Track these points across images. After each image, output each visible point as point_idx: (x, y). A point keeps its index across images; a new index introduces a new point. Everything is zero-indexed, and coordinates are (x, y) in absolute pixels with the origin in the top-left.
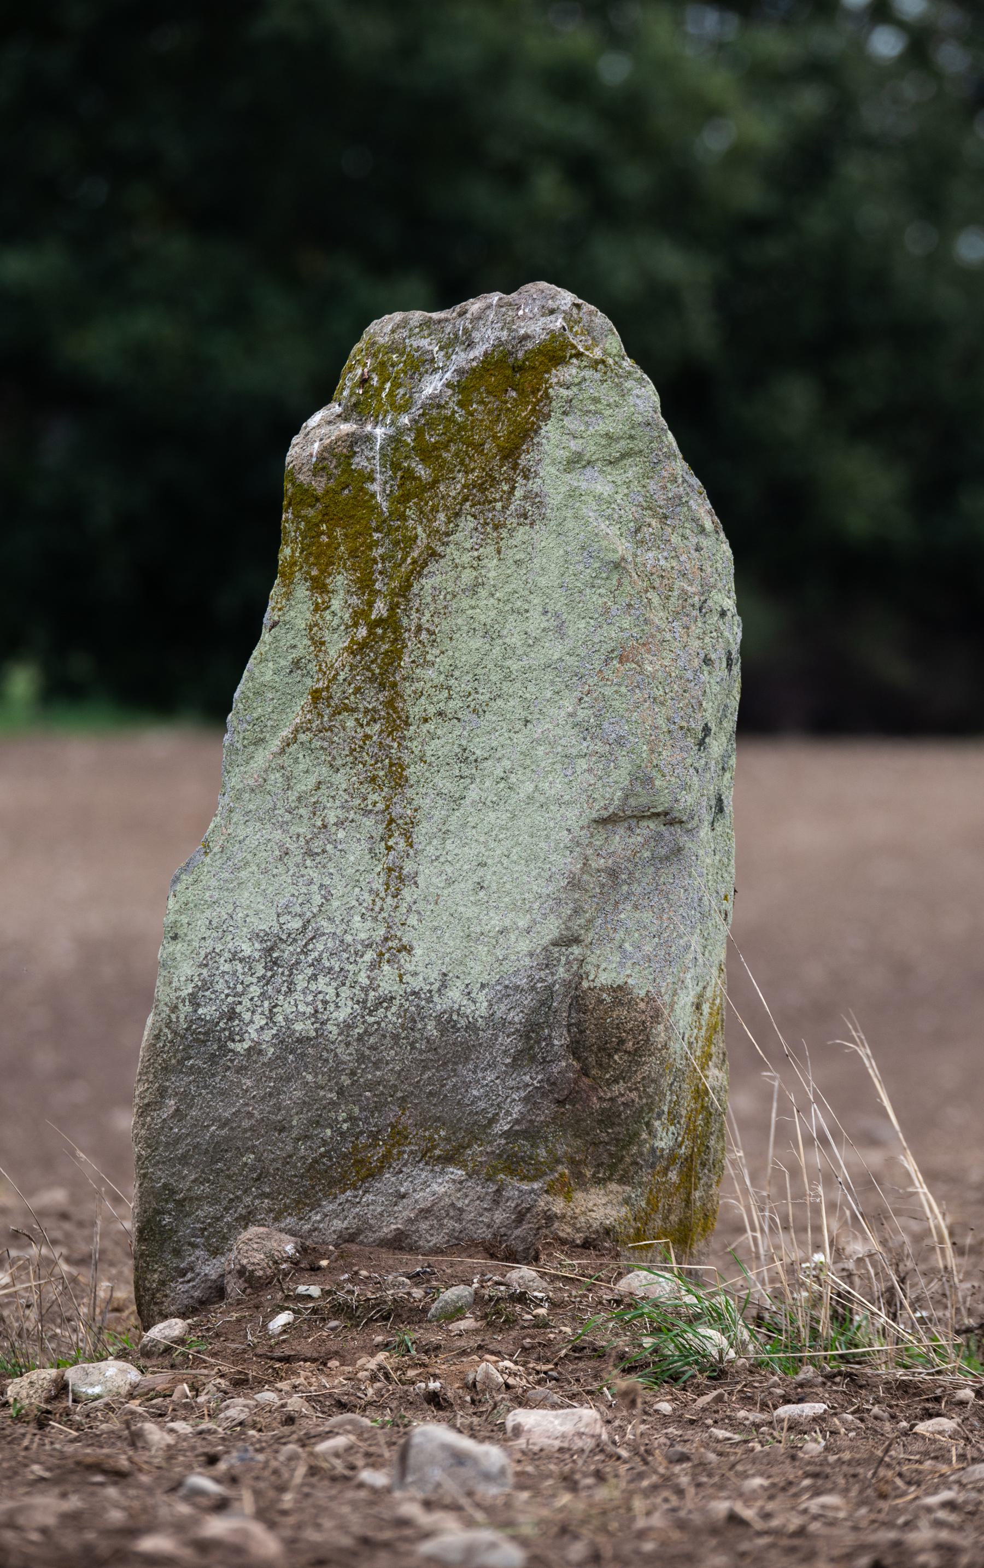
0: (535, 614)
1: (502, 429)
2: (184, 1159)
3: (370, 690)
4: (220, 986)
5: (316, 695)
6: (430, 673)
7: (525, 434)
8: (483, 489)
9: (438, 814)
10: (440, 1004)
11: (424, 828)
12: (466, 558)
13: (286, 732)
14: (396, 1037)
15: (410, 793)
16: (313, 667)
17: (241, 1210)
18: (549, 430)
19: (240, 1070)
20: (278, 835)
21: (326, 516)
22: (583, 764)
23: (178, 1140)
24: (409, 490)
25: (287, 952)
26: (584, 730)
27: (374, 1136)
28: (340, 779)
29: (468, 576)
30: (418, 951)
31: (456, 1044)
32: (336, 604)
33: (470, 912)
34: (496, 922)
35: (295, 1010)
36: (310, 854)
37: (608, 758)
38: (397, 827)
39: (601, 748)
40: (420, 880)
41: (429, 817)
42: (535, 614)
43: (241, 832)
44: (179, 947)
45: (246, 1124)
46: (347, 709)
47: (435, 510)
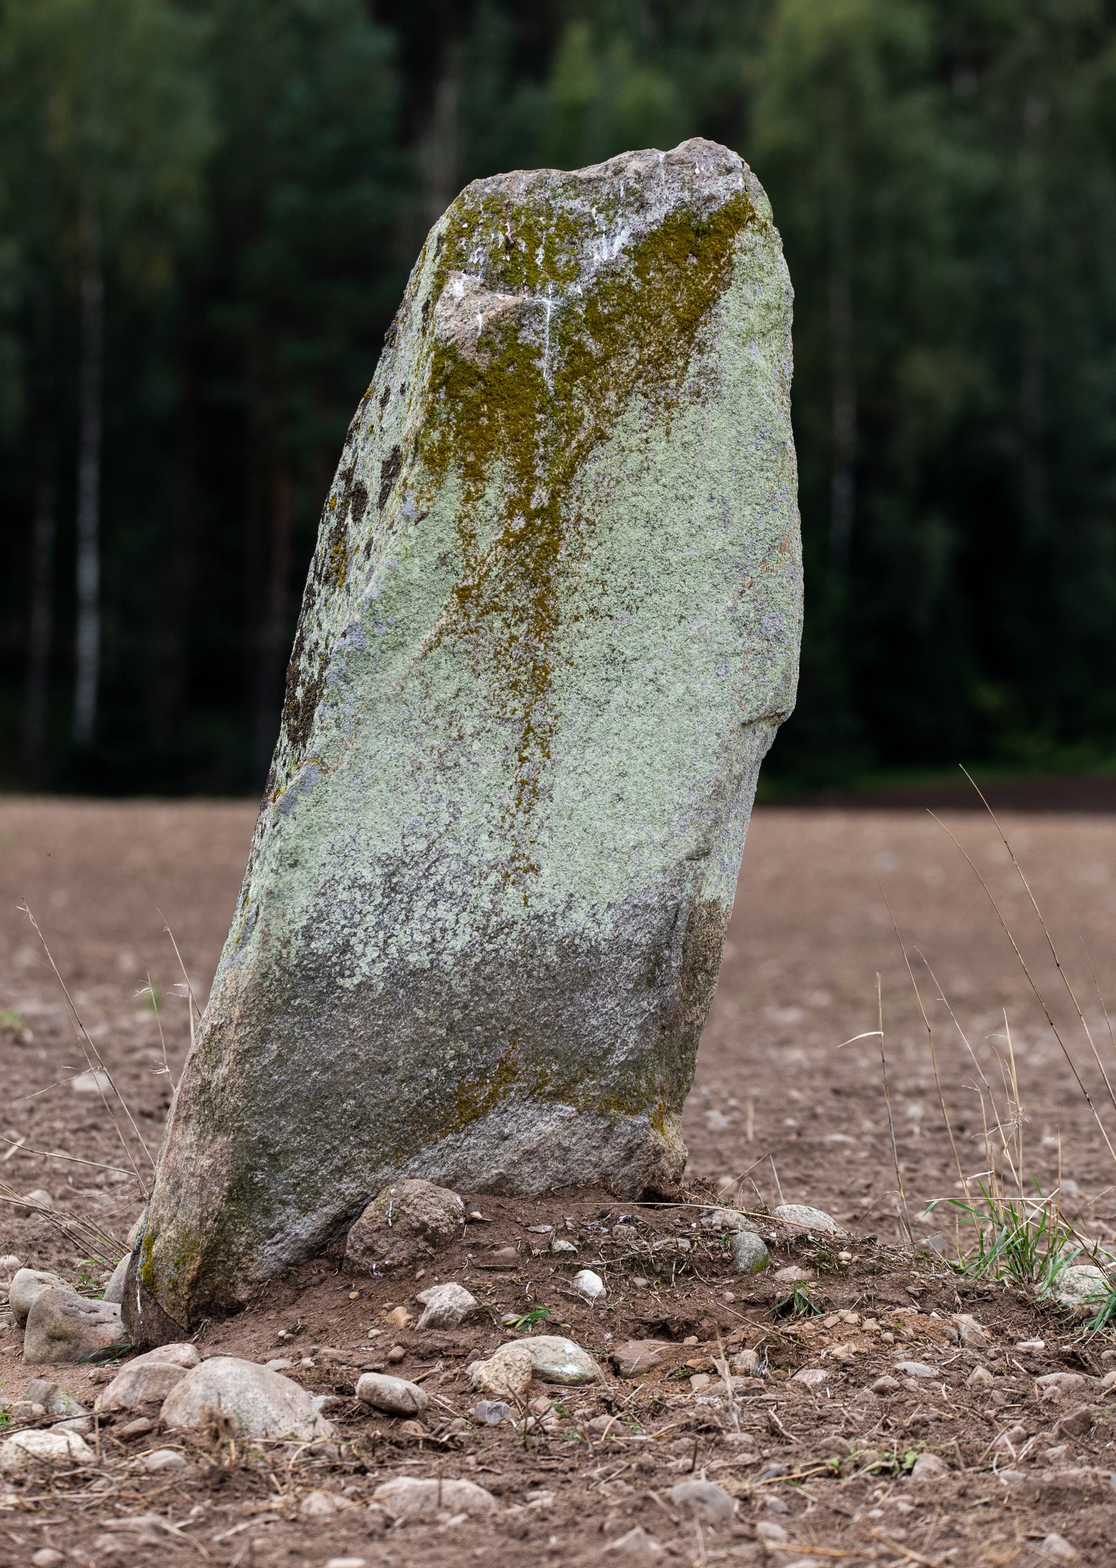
0: (701, 501)
1: (681, 299)
2: (282, 1110)
3: (521, 588)
4: (337, 916)
5: (463, 594)
6: (585, 567)
7: (705, 303)
8: (657, 365)
9: (580, 721)
10: (563, 928)
11: (565, 736)
12: (634, 441)
13: (429, 635)
14: (513, 965)
15: (552, 698)
16: (459, 563)
17: (338, 1162)
18: (728, 298)
19: (348, 1008)
20: (410, 748)
21: (488, 396)
22: (737, 662)
23: (278, 1087)
24: (578, 366)
25: (408, 877)
26: (743, 626)
27: (482, 1074)
28: (480, 686)
29: (634, 461)
30: (546, 871)
31: (577, 970)
32: (491, 493)
33: (605, 826)
34: (631, 837)
35: (410, 940)
36: (442, 768)
37: (766, 656)
38: (535, 736)
39: (758, 644)
40: (556, 794)
41: (570, 724)
42: (701, 501)
43: (373, 746)
44: (298, 874)
45: (350, 1067)
46: (497, 608)
47: (605, 388)
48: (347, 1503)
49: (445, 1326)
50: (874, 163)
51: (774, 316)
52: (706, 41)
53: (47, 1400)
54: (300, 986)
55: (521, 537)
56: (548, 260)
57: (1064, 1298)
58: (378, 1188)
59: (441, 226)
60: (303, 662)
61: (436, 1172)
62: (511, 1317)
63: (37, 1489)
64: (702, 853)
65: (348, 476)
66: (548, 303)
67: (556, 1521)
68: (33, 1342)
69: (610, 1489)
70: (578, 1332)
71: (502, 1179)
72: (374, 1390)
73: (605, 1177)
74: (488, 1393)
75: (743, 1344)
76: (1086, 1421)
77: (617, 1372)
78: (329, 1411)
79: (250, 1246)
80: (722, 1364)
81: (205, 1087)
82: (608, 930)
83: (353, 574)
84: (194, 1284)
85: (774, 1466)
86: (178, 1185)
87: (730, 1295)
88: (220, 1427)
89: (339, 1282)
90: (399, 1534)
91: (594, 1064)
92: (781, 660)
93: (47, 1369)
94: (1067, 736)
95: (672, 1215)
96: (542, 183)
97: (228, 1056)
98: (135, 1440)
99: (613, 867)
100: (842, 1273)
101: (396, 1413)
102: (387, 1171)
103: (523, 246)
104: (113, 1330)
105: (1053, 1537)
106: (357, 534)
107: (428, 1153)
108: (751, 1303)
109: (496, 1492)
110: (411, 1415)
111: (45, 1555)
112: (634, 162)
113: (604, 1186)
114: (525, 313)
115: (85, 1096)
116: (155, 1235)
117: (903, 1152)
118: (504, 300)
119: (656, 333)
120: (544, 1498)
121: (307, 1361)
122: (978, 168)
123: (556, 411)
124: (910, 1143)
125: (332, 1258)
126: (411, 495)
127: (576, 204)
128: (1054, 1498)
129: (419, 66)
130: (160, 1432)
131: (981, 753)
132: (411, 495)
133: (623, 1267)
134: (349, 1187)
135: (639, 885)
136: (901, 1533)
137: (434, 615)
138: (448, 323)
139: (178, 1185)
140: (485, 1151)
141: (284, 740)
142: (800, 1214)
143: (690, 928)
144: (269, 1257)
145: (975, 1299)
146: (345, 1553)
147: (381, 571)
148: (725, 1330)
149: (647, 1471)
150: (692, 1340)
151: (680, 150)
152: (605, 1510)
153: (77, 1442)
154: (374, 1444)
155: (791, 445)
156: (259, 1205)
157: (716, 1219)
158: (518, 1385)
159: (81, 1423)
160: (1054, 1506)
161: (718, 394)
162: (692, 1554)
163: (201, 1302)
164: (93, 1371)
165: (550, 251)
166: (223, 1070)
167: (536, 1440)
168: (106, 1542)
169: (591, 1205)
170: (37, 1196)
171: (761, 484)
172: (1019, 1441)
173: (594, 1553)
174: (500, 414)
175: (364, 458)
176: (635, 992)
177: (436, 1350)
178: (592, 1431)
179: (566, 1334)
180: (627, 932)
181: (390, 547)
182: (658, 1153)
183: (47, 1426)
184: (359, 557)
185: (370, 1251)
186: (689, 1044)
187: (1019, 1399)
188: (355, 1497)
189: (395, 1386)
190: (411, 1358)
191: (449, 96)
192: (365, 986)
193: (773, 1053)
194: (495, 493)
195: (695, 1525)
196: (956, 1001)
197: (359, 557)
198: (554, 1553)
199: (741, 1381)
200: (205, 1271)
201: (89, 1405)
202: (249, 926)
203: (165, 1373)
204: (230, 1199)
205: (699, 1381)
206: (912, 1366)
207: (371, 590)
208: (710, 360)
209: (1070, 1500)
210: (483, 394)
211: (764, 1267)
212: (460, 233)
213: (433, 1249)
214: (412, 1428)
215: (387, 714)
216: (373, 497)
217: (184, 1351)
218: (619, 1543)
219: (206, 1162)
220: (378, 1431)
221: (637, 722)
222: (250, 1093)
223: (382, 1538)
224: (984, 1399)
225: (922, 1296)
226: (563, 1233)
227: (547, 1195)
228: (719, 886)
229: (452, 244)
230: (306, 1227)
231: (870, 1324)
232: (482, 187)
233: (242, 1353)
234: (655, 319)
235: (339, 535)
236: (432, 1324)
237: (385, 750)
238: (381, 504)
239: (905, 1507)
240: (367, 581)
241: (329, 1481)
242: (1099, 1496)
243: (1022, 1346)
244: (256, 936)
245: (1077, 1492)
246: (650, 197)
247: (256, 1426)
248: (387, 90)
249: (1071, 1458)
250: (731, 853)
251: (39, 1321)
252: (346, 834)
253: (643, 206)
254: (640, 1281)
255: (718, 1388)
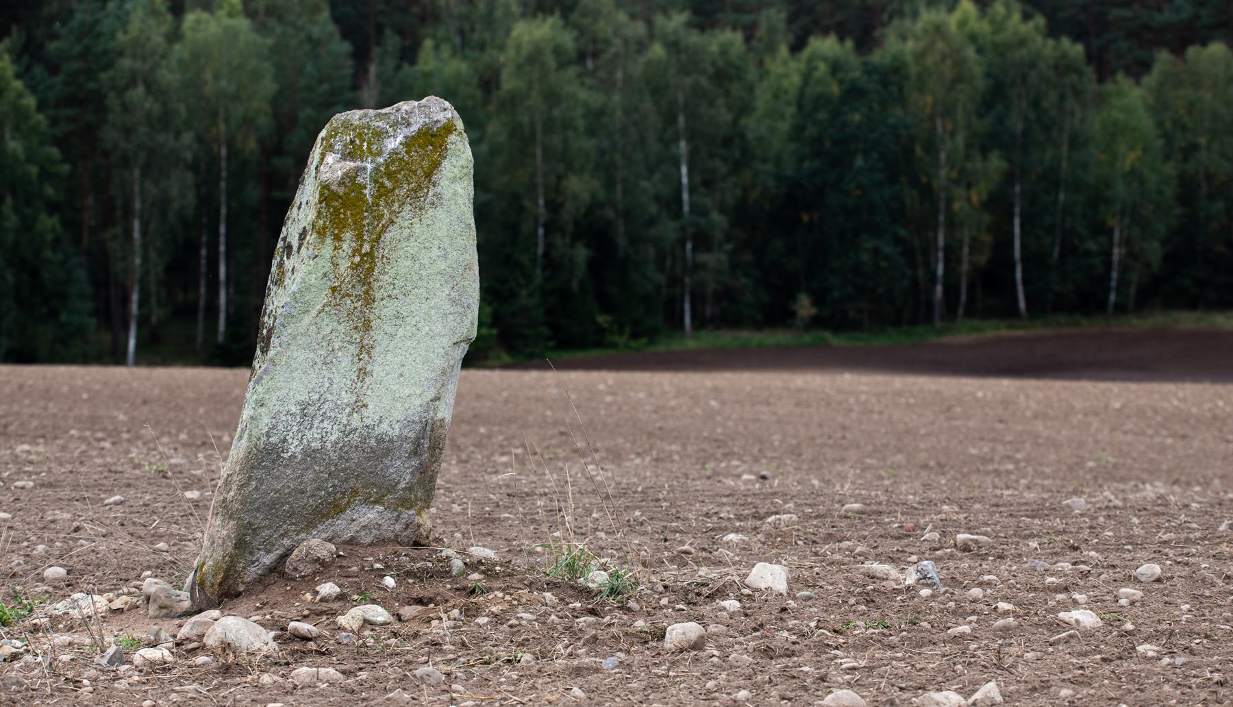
0: (435, 249)
1: (425, 164)
2: (258, 510)
3: (358, 287)
4: (280, 427)
5: (334, 289)
6: (386, 277)
7: (436, 165)
8: (416, 192)
9: (385, 343)
10: (378, 431)
11: (378, 349)
12: (406, 224)
13: (319, 307)
14: (357, 447)
15: (372, 333)
16: (332, 276)
17: (282, 532)
18: (445, 163)
19: (286, 466)
20: (312, 355)
21: (343, 205)
22: (451, 317)
23: (256, 500)
24: (382, 192)
25: (311, 410)
26: (453, 302)
27: (343, 493)
28: (342, 328)
29: (406, 232)
30: (370, 407)
31: (384, 449)
32: (345, 246)
33: (395, 387)
34: (407, 392)
35: (312, 437)
36: (325, 364)
37: (463, 314)
38: (365, 349)
39: (460, 310)
40: (374, 374)
41: (380, 344)
42: (435, 249)
43: (295, 354)
44: (264, 409)
45: (287, 491)
46: (348, 295)
47: (393, 201)
48: (279, 678)
49: (327, 601)
50: (552, 97)
51: (465, 170)
52: (482, 47)
53: (157, 634)
54: (265, 457)
55: (358, 265)
56: (368, 148)
57: (590, 585)
58: (299, 542)
59: (323, 133)
60: (266, 319)
61: (324, 535)
62: (355, 597)
63: (148, 673)
64: (437, 399)
65: (284, 239)
66: (369, 166)
67: (367, 685)
68: (152, 609)
69: (392, 671)
70: (384, 603)
71: (353, 538)
72: (296, 629)
73: (396, 536)
74: (344, 629)
75: (454, 607)
76: (595, 638)
77: (400, 620)
78: (276, 638)
79: (244, 568)
80: (443, 615)
81: (224, 501)
82: (397, 432)
83: (287, 281)
84: (220, 584)
85: (462, 660)
86: (213, 542)
87: (449, 586)
88: (226, 647)
89: (282, 582)
90: (299, 692)
91: (392, 488)
92: (470, 316)
93: (158, 621)
94: (635, 336)
95: (425, 552)
96: (366, 115)
97: (234, 487)
98: (193, 652)
99: (399, 405)
100: (497, 576)
101: (305, 639)
102: (303, 535)
103: (358, 142)
104: (187, 604)
105: (575, 689)
106: (289, 264)
107: (321, 527)
108: (457, 589)
109: (344, 673)
110: (310, 640)
111: (148, 703)
112: (404, 106)
113: (396, 540)
114: (359, 170)
115: (189, 500)
116: (204, 564)
117: (533, 521)
118: (350, 164)
119: (415, 179)
120: (363, 675)
121: (268, 617)
122: (596, 99)
123: (373, 211)
124: (537, 517)
125: (279, 573)
126: (311, 248)
127: (380, 124)
128: (578, 672)
129: (361, 56)
130: (203, 648)
131: (599, 344)
132: (311, 248)
133: (403, 575)
134: (287, 542)
135: (410, 412)
136: (513, 688)
137: (323, 298)
138: (326, 175)
139: (213, 542)
140: (344, 526)
141: (258, 352)
142: (480, 551)
143: (432, 430)
144: (253, 572)
145: (552, 586)
146: (275, 701)
147: (298, 280)
148: (447, 601)
149: (409, 663)
150: (432, 606)
151: (424, 101)
152: (388, 680)
153: (166, 653)
154: (293, 653)
155: (473, 225)
156: (248, 550)
157: (443, 554)
158: (355, 627)
159: (170, 645)
160: (578, 675)
161: (442, 204)
162: (422, 699)
163: (223, 592)
164: (177, 622)
165: (370, 144)
166: (232, 493)
167: (363, 650)
168: (174, 697)
169: (390, 549)
170: (162, 545)
171: (460, 242)
172: (567, 647)
173: (380, 700)
174: (348, 213)
175: (291, 231)
176: (408, 458)
177: (324, 611)
178: (387, 645)
179: (378, 604)
180: (405, 432)
181: (302, 270)
182: (419, 526)
183: (155, 646)
184: (289, 274)
185: (296, 569)
186: (432, 479)
187: (568, 629)
188: (283, 676)
189: (305, 627)
190: (313, 615)
191: (373, 69)
192: (293, 456)
193: (486, 477)
194: (347, 246)
195: (424, 686)
196: (575, 451)
197: (289, 274)
198: (364, 699)
199: (451, 623)
200: (225, 579)
201: (174, 636)
202: (243, 431)
203: (205, 623)
204: (235, 548)
205: (435, 623)
206: (525, 615)
207: (294, 288)
208: (438, 189)
209: (584, 672)
210: (342, 205)
211: (463, 574)
212: (331, 137)
213: (323, 568)
214: (312, 645)
215: (301, 340)
216: (295, 249)
217: (215, 613)
218: (390, 695)
219: (225, 532)
220: (296, 646)
221: (409, 343)
222: (243, 503)
223: (292, 694)
224: (554, 629)
225: (530, 585)
226: (378, 561)
227: (372, 544)
228: (445, 412)
229: (328, 141)
230: (268, 559)
231: (508, 597)
232: (340, 117)
233: (241, 614)
234: (415, 172)
235: (281, 265)
236: (322, 600)
237: (301, 356)
238: (298, 252)
239: (515, 677)
240: (292, 284)
241: (273, 669)
242: (597, 670)
243: (571, 606)
244: (246, 436)
245: (587, 669)
246: (412, 121)
247: (244, 645)
248: (348, 67)
249: (587, 654)
250: (449, 398)
251: (155, 601)
252: (284, 392)
253: (409, 125)
254: (411, 581)
255: (442, 626)
